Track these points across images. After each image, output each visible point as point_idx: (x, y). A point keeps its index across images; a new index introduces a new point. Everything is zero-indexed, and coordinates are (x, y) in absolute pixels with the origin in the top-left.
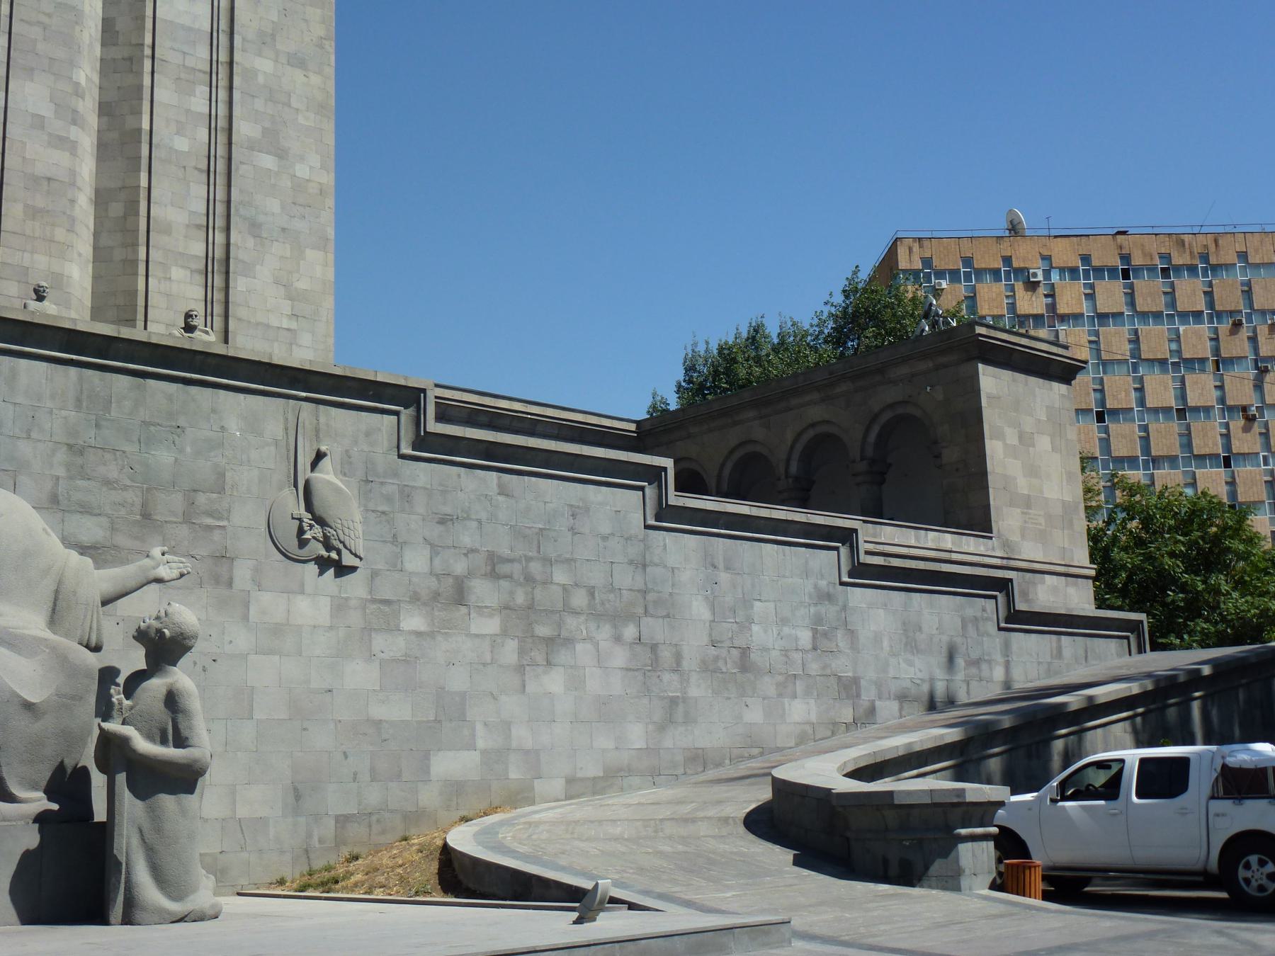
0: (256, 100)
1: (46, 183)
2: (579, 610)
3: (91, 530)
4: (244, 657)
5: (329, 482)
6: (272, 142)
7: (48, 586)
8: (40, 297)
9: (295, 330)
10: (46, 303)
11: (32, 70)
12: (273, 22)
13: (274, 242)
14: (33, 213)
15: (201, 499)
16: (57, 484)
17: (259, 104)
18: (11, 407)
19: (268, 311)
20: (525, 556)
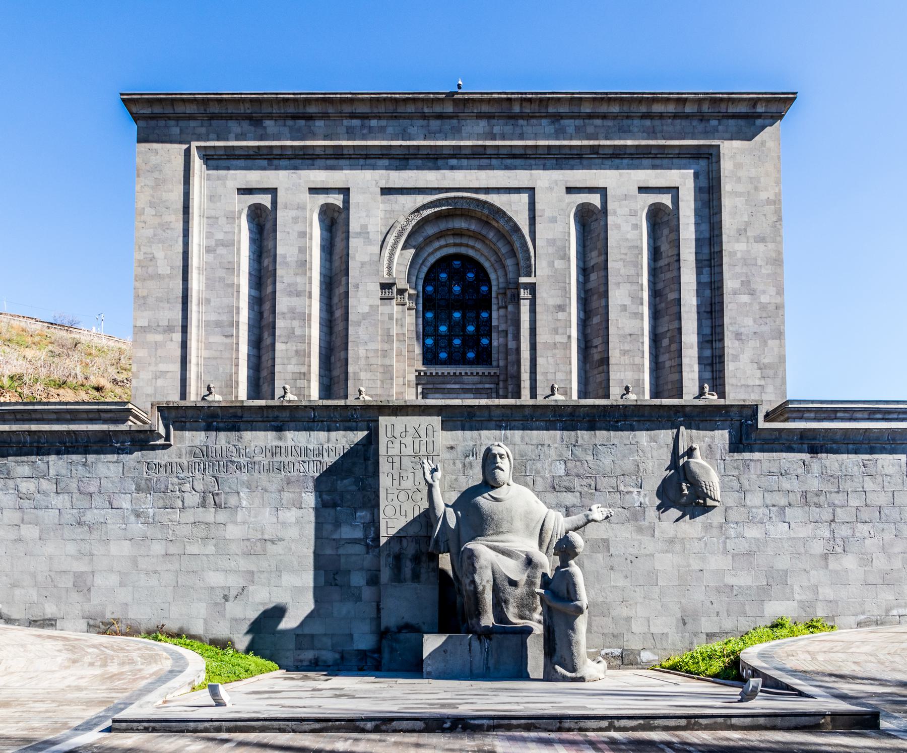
11: (619, 283)
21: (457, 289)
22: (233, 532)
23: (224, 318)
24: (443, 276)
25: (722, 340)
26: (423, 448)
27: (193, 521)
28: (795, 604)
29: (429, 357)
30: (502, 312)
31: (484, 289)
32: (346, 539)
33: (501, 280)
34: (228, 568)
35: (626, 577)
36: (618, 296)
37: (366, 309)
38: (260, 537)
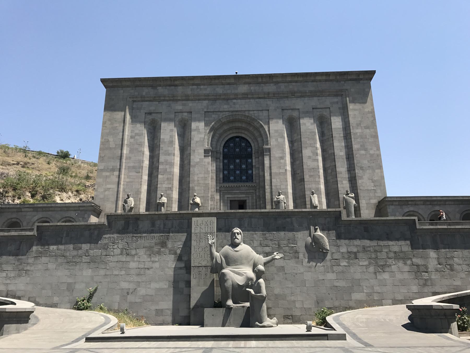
0: (358, 139)
1: (312, 169)
2: (392, 257)
3: (268, 249)
4: (302, 273)
5: (318, 234)
6: (363, 147)
7: (252, 262)
8: (313, 194)
9: (375, 189)
10: (315, 195)
11: (307, 147)
12: (360, 121)
13: (367, 170)
14: (311, 176)
15: (290, 241)
16: (261, 241)
17: (359, 140)
18: (251, 228)
19: (368, 186)
20: (374, 246)
21: (237, 150)
22: (133, 265)
23: (137, 165)
24: (232, 145)
25: (354, 170)
26: (209, 230)
27: (117, 261)
28: (365, 294)
29: (226, 179)
30: (257, 159)
31: (249, 150)
32: (178, 267)
33: (256, 146)
34: (130, 281)
35: (292, 283)
36: (306, 152)
37: (198, 160)
38: (143, 267)
